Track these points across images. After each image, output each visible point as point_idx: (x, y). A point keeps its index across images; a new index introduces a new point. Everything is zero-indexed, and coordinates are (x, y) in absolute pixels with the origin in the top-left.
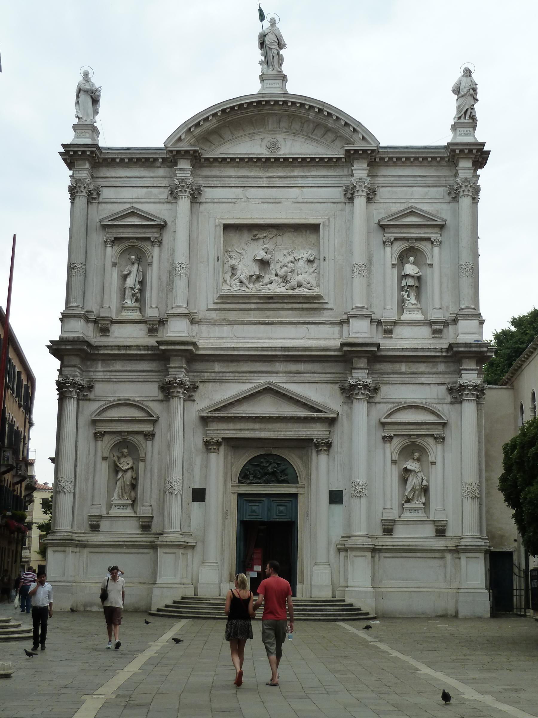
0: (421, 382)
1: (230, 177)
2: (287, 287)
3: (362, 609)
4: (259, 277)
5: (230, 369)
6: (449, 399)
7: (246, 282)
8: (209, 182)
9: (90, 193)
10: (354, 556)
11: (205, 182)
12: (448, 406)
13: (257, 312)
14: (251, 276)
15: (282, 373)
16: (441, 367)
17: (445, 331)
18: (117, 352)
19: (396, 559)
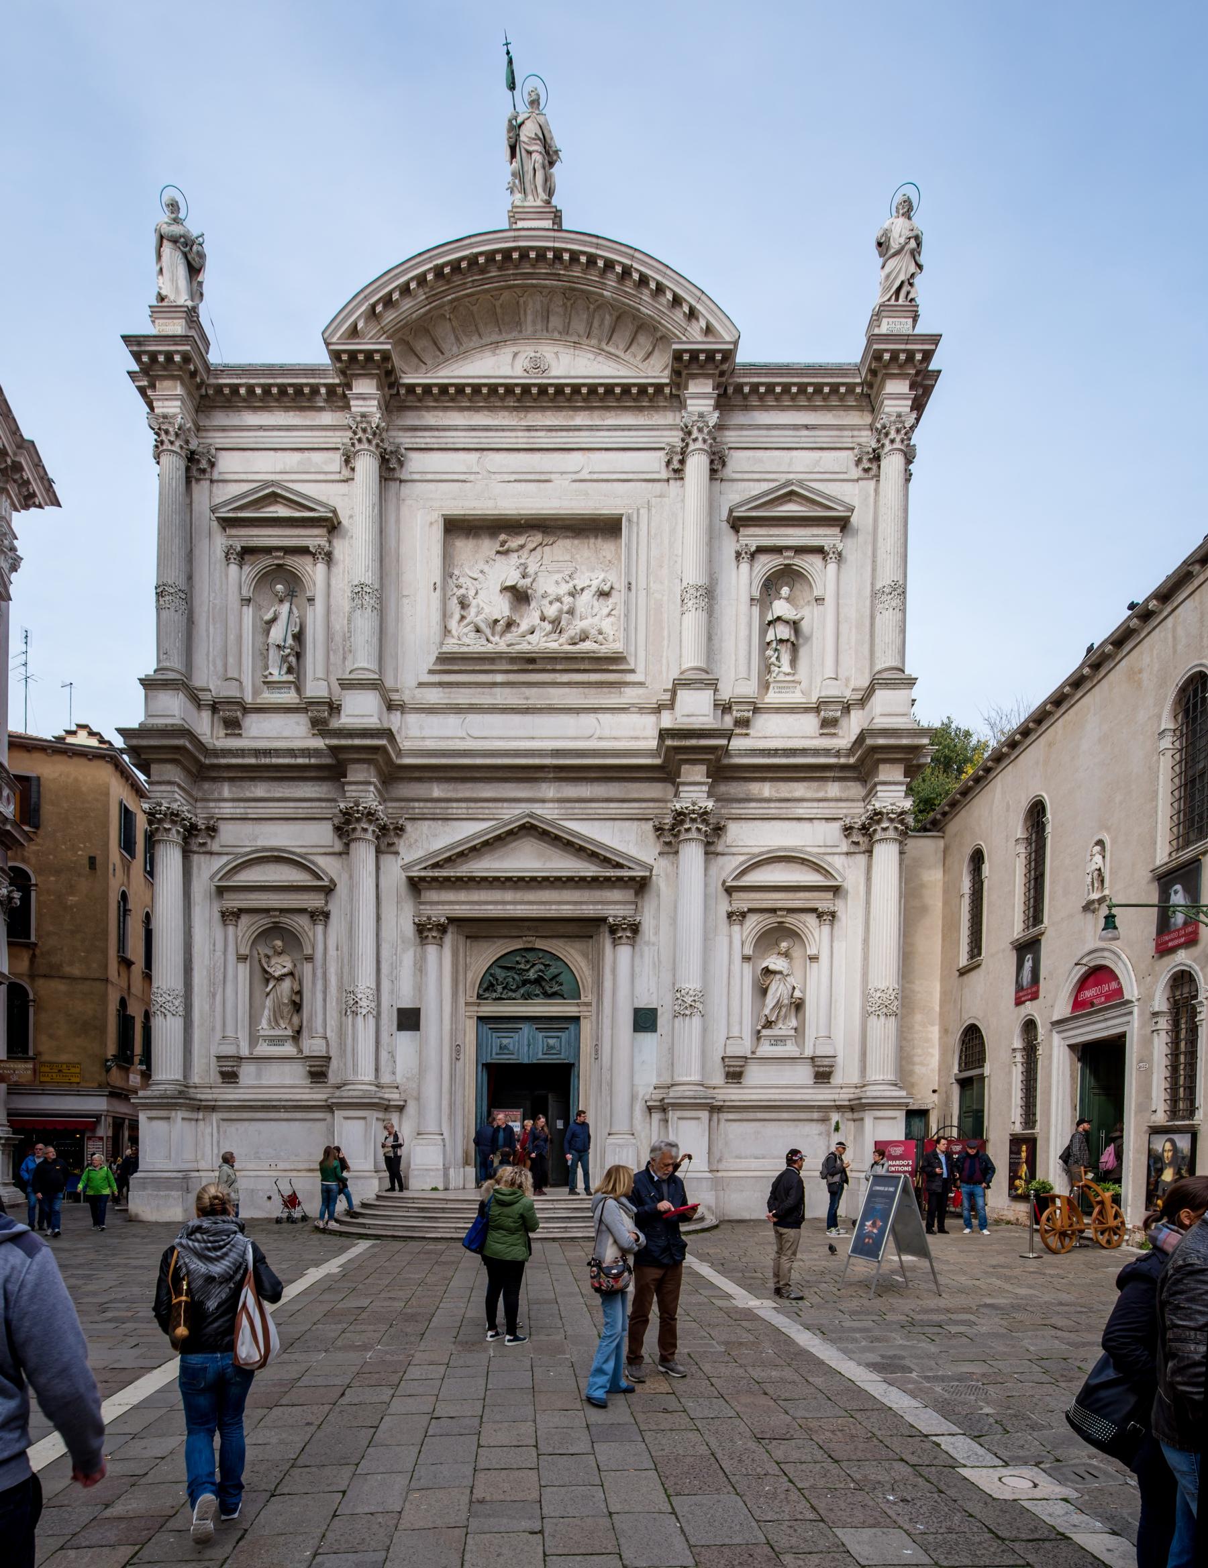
1: (455, 428)
2: (562, 640)
4: (510, 624)
5: (460, 795)
6: (845, 846)
7: (488, 631)
8: (418, 440)
9: (192, 457)
12: (843, 857)
13: (507, 691)
14: (496, 621)
15: (552, 801)
16: (834, 789)
17: (844, 722)
18: (252, 761)
19: (745, 1124)
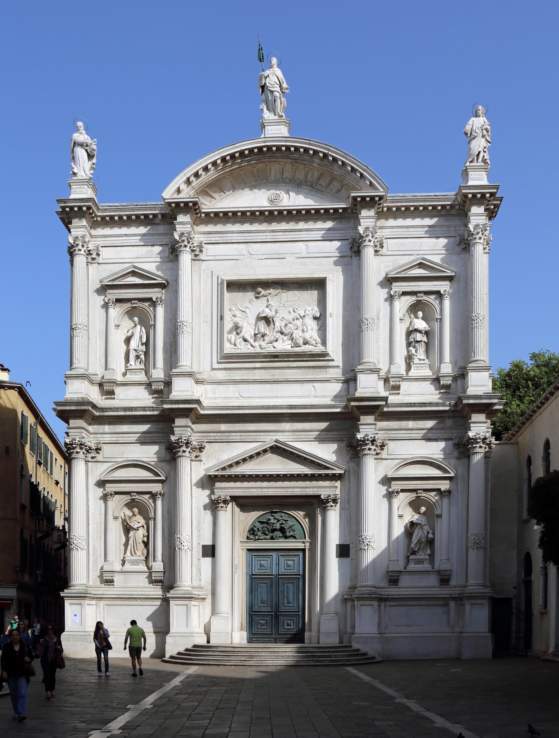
1: (232, 232)
3: (369, 653)
10: (361, 605)
11: (206, 239)
18: (122, 413)
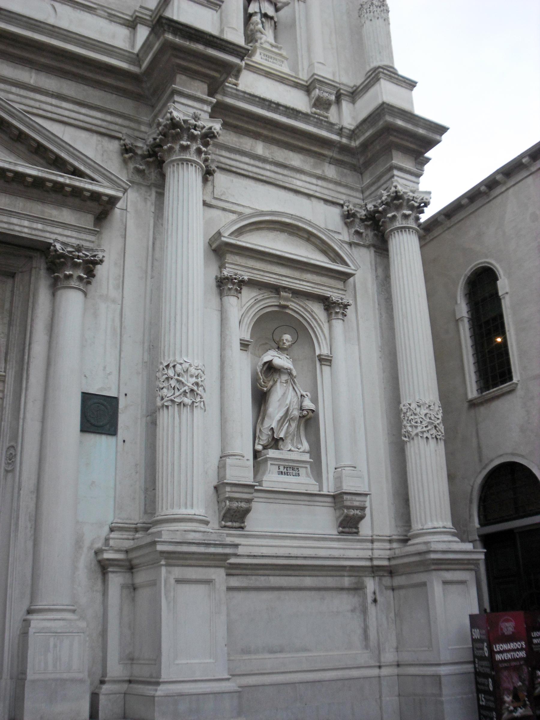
0: (294, 187)
19: (253, 595)
